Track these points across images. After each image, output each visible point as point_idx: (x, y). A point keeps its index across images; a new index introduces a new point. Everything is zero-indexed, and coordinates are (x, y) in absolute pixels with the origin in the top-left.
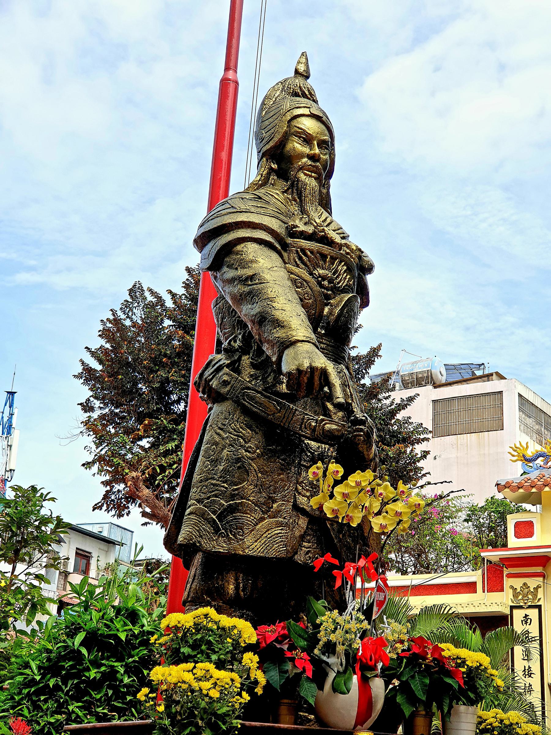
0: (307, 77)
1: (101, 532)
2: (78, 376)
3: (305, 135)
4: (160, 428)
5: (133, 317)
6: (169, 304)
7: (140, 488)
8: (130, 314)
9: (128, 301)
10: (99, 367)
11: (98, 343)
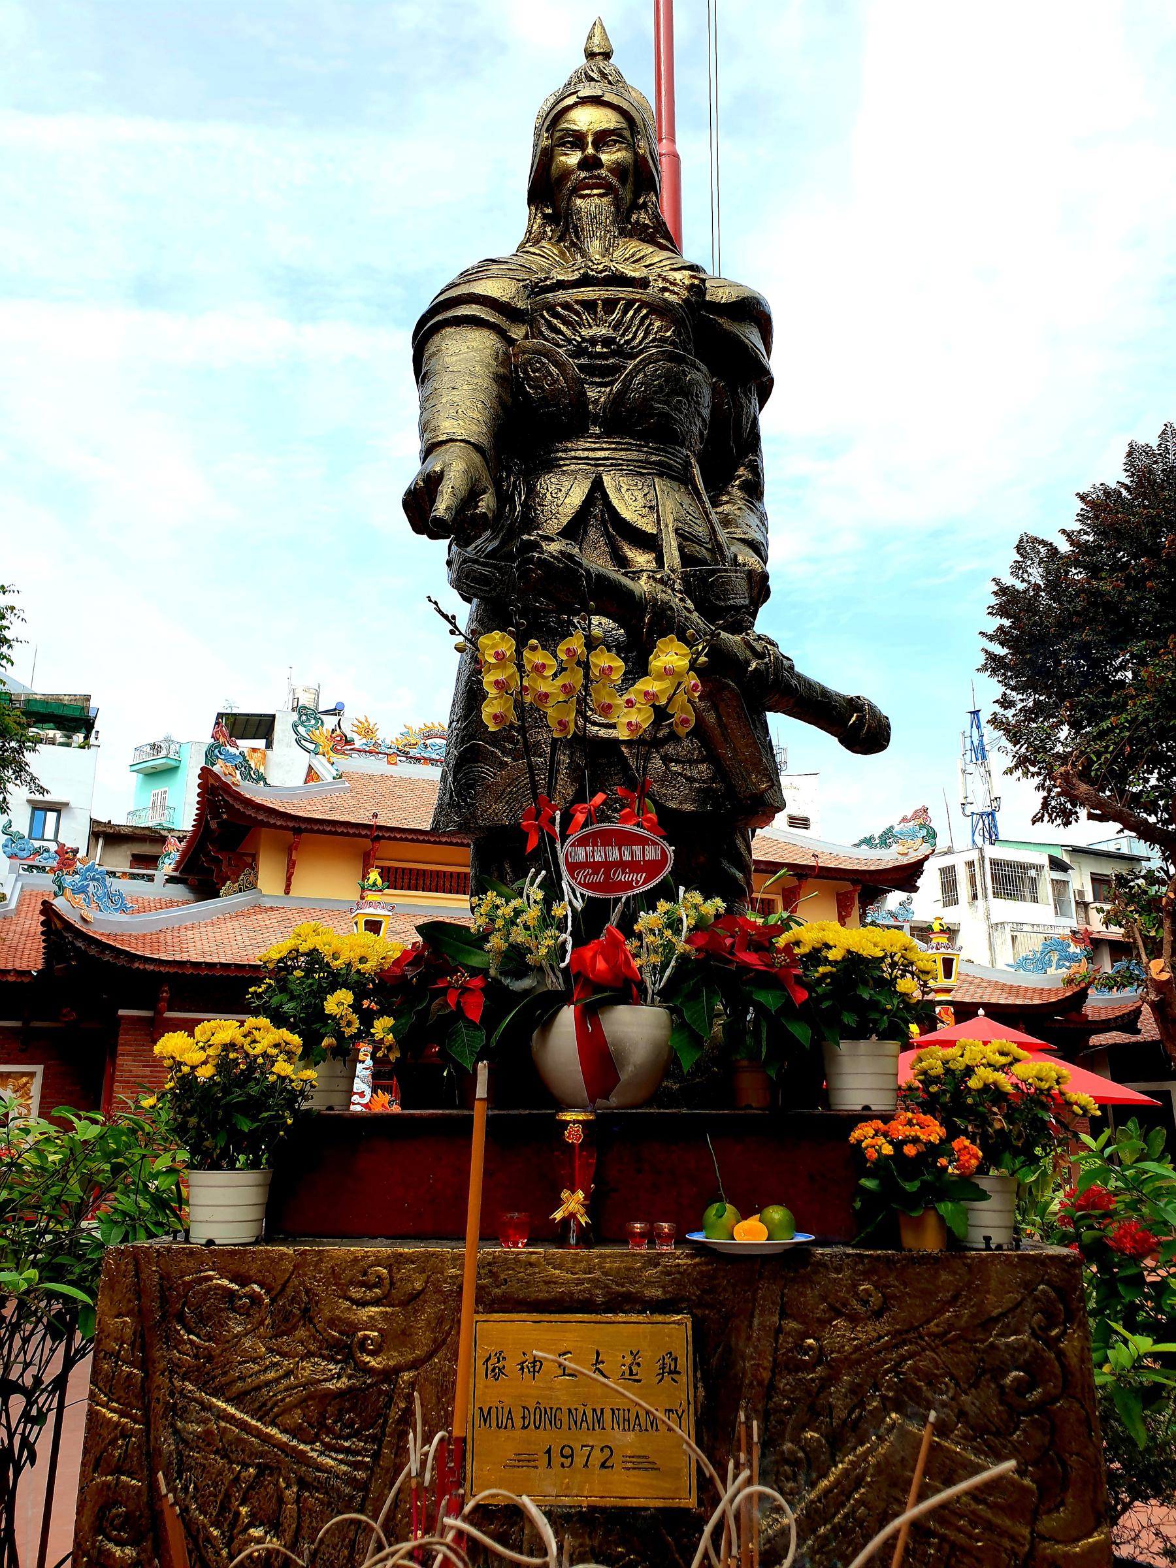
0: (607, 55)
1: (1119, 849)
2: (984, 668)
3: (572, 136)
5: (1031, 578)
6: (1064, 547)
7: (1074, 785)
8: (1025, 576)
9: (1018, 562)
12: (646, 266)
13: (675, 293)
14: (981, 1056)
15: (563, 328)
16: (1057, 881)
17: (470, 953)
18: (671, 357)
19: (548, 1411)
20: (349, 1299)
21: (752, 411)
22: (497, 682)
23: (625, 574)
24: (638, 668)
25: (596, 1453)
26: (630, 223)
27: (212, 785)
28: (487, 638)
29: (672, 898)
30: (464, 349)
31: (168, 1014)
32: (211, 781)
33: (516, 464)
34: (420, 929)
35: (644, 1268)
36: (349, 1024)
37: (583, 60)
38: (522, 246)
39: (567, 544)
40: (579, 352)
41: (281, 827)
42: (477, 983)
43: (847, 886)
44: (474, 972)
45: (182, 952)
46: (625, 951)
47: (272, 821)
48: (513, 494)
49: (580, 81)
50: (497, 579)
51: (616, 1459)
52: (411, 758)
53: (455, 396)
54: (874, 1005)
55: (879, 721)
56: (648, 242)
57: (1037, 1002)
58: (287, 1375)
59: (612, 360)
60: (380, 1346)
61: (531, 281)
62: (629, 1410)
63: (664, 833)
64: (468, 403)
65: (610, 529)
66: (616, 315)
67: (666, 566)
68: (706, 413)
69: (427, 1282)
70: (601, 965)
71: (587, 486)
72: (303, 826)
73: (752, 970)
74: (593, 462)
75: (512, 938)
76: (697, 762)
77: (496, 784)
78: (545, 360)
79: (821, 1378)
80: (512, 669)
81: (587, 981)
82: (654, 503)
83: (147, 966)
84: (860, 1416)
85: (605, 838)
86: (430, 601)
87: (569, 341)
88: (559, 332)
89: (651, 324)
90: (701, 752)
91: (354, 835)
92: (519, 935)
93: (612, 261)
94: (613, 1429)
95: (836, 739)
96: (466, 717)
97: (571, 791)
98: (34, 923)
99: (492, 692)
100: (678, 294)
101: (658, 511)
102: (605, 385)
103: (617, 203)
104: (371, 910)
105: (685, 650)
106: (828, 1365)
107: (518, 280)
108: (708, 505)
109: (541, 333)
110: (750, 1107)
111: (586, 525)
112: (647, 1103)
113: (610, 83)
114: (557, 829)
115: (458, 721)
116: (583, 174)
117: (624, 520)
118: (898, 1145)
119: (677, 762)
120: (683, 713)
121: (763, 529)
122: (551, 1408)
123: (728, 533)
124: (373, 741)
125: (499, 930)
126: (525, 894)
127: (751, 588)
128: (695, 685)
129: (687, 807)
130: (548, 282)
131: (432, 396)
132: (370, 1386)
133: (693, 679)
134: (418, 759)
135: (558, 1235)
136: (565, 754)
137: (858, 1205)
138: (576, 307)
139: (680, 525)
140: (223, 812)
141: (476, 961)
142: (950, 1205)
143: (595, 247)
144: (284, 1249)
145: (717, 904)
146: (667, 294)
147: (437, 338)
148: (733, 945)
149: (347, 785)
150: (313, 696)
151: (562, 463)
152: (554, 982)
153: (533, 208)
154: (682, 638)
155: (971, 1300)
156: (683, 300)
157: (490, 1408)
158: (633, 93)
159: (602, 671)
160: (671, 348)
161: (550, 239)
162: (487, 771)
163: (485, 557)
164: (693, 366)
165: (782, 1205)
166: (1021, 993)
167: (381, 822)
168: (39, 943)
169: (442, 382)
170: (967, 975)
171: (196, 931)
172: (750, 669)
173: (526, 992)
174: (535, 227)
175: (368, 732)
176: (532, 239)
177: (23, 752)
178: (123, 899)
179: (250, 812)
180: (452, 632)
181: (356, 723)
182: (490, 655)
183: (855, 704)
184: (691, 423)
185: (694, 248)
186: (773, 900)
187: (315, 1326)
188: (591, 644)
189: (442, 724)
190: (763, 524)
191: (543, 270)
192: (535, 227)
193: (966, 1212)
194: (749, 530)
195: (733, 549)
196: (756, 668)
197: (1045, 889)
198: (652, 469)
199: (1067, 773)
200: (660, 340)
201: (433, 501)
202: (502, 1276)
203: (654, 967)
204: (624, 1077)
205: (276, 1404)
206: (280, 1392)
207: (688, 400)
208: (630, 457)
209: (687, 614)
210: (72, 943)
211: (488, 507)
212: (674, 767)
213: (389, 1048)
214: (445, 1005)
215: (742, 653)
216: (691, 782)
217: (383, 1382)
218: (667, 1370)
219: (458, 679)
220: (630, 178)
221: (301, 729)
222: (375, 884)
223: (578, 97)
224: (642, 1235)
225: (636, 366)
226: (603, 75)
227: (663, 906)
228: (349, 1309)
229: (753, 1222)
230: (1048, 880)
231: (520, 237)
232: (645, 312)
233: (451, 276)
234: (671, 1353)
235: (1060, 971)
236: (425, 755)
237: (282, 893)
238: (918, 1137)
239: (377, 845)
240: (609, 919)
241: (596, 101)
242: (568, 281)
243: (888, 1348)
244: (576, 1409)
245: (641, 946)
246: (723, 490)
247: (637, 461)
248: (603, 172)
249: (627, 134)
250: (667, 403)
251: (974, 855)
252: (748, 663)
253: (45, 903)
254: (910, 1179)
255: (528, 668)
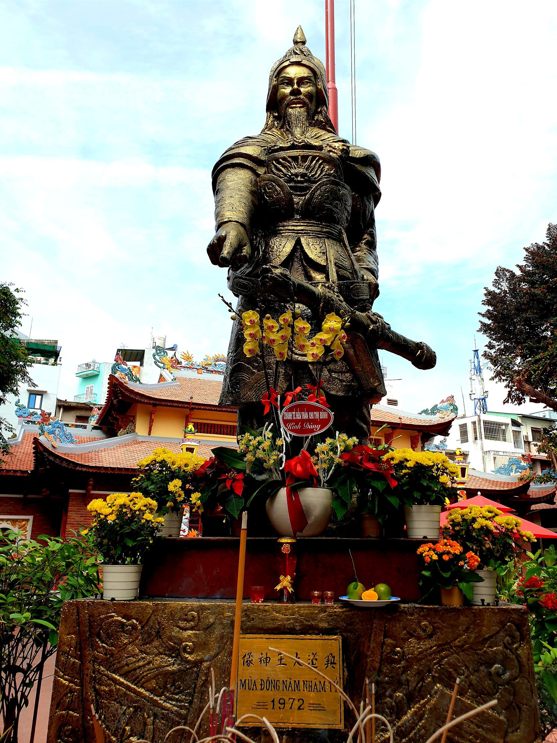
0: (304, 43)
1: (545, 416)
2: (480, 330)
4: (529, 348)
5: (502, 287)
6: (518, 273)
7: (523, 385)
8: (500, 286)
9: (496, 280)
10: (490, 322)
11: (485, 309)
12: (322, 140)
13: (335, 153)
14: (479, 513)
15: (283, 169)
16: (515, 431)
17: (237, 462)
18: (333, 183)
19: (273, 681)
20: (179, 627)
21: (371, 208)
22: (250, 334)
23: (311, 284)
24: (317, 328)
25: (296, 702)
26: (314, 120)
27: (115, 383)
28: (246, 314)
29: (333, 437)
30: (236, 179)
31: (93, 492)
32: (114, 381)
33: (260, 232)
34: (213, 450)
35: (319, 613)
36: (180, 496)
37: (292, 45)
38: (263, 130)
39: (284, 270)
40: (290, 180)
41: (147, 403)
42: (240, 476)
43: (416, 433)
44: (239, 471)
45: (99, 462)
46: (310, 462)
47: (143, 400)
48: (259, 247)
49: (291, 55)
50: (251, 286)
51: (305, 705)
52: (209, 370)
53: (232, 201)
54: (429, 488)
55: (431, 354)
56: (322, 129)
57: (506, 489)
58: (149, 663)
59: (306, 184)
60: (194, 649)
61: (268, 147)
62: (311, 681)
63: (329, 406)
64: (238, 204)
65: (304, 263)
66: (307, 163)
67: (330, 280)
68: (349, 209)
69: (215, 619)
70: (299, 468)
71: (293, 242)
72: (157, 403)
73: (371, 471)
74: (296, 232)
75: (257, 455)
76: (345, 372)
77: (250, 382)
78: (274, 184)
79: (404, 667)
80: (258, 328)
81: (293, 476)
82: (325, 251)
83: (83, 469)
84: (422, 686)
85: (301, 408)
86: (220, 296)
87: (285, 175)
88: (280, 171)
89: (324, 167)
90: (346, 368)
91: (181, 407)
92: (260, 454)
93: (305, 138)
94: (304, 690)
95: (411, 362)
96: (236, 351)
97: (285, 386)
98: (30, 448)
99: (248, 339)
100: (336, 153)
101: (326, 255)
102: (302, 196)
103: (308, 111)
104: (189, 443)
105: (339, 319)
106: (407, 660)
107: (262, 147)
108: (350, 252)
109: (272, 171)
110: (370, 537)
111: (293, 261)
112: (321, 534)
113: (305, 55)
114: (279, 404)
115: (232, 353)
116: (292, 97)
117: (311, 258)
118: (440, 555)
119: (335, 372)
120: (338, 349)
121: (376, 263)
122: (275, 680)
123: (359, 265)
124: (191, 363)
125: (251, 451)
126: (263, 435)
127: (370, 291)
128: (344, 336)
129: (340, 394)
130: (276, 148)
131: (221, 201)
132: (188, 669)
133: (343, 333)
134: (212, 371)
135: (278, 597)
136: (282, 368)
137: (421, 584)
138: (289, 159)
139: (337, 261)
140: (119, 396)
141: (240, 466)
142: (465, 584)
143: (297, 132)
144: (148, 603)
145: (354, 440)
146: (331, 153)
147: (223, 174)
148: (362, 459)
149: (178, 383)
150: (163, 341)
151: (282, 232)
152: (276, 476)
153: (269, 113)
154: (338, 314)
155: (475, 630)
156: (339, 156)
157: (245, 680)
158: (315, 60)
159: (300, 329)
160: (333, 179)
161: (277, 127)
162: (245, 376)
163: (245, 276)
164: (343, 187)
165: (384, 583)
166: (499, 484)
167: (195, 401)
168: (32, 458)
169: (226, 194)
170: (472, 476)
171: (106, 452)
172: (370, 329)
173: (263, 481)
174: (270, 122)
175: (188, 358)
176: (268, 127)
177: (25, 367)
178: (72, 437)
179: (132, 396)
180: (230, 311)
181: (183, 354)
182: (247, 321)
183: (419, 346)
184: (342, 213)
185: (344, 132)
186: (380, 440)
187: (162, 640)
188: (295, 316)
189: (223, 354)
190: (376, 261)
191: (273, 142)
192: (270, 122)
193: (472, 588)
194: (369, 264)
195: (362, 272)
196: (373, 328)
197: (510, 435)
198: (324, 235)
199: (520, 379)
200: (328, 175)
201: (221, 249)
202: (252, 616)
203: (324, 470)
204: (310, 522)
205: (143, 677)
206: (146, 671)
207: (341, 203)
208: (313, 229)
209: (340, 303)
210: (47, 458)
211: (247, 253)
212: (334, 375)
213: (199, 507)
214: (225, 487)
215: (366, 321)
216: (342, 382)
217: (194, 667)
218: (330, 662)
219: (232, 333)
220: (314, 99)
221: (157, 357)
222: (191, 431)
223: (290, 62)
224: (318, 597)
225: (316, 187)
226: (302, 52)
227: (329, 440)
228: (179, 632)
229: (371, 591)
230: (511, 431)
231: (263, 126)
232: (321, 161)
233: (230, 144)
234: (332, 654)
235: (517, 474)
236: (215, 369)
237: (147, 435)
238: (450, 552)
239: (192, 412)
240: (302, 447)
241: (298, 64)
242: (285, 147)
243: (435, 652)
244: (286, 681)
245: (318, 460)
246: (357, 245)
247: (317, 231)
248: (302, 97)
249: (313, 79)
250: (331, 204)
251: (476, 419)
252: (369, 326)
253: (35, 438)
254: (446, 572)
255: (265, 327)
